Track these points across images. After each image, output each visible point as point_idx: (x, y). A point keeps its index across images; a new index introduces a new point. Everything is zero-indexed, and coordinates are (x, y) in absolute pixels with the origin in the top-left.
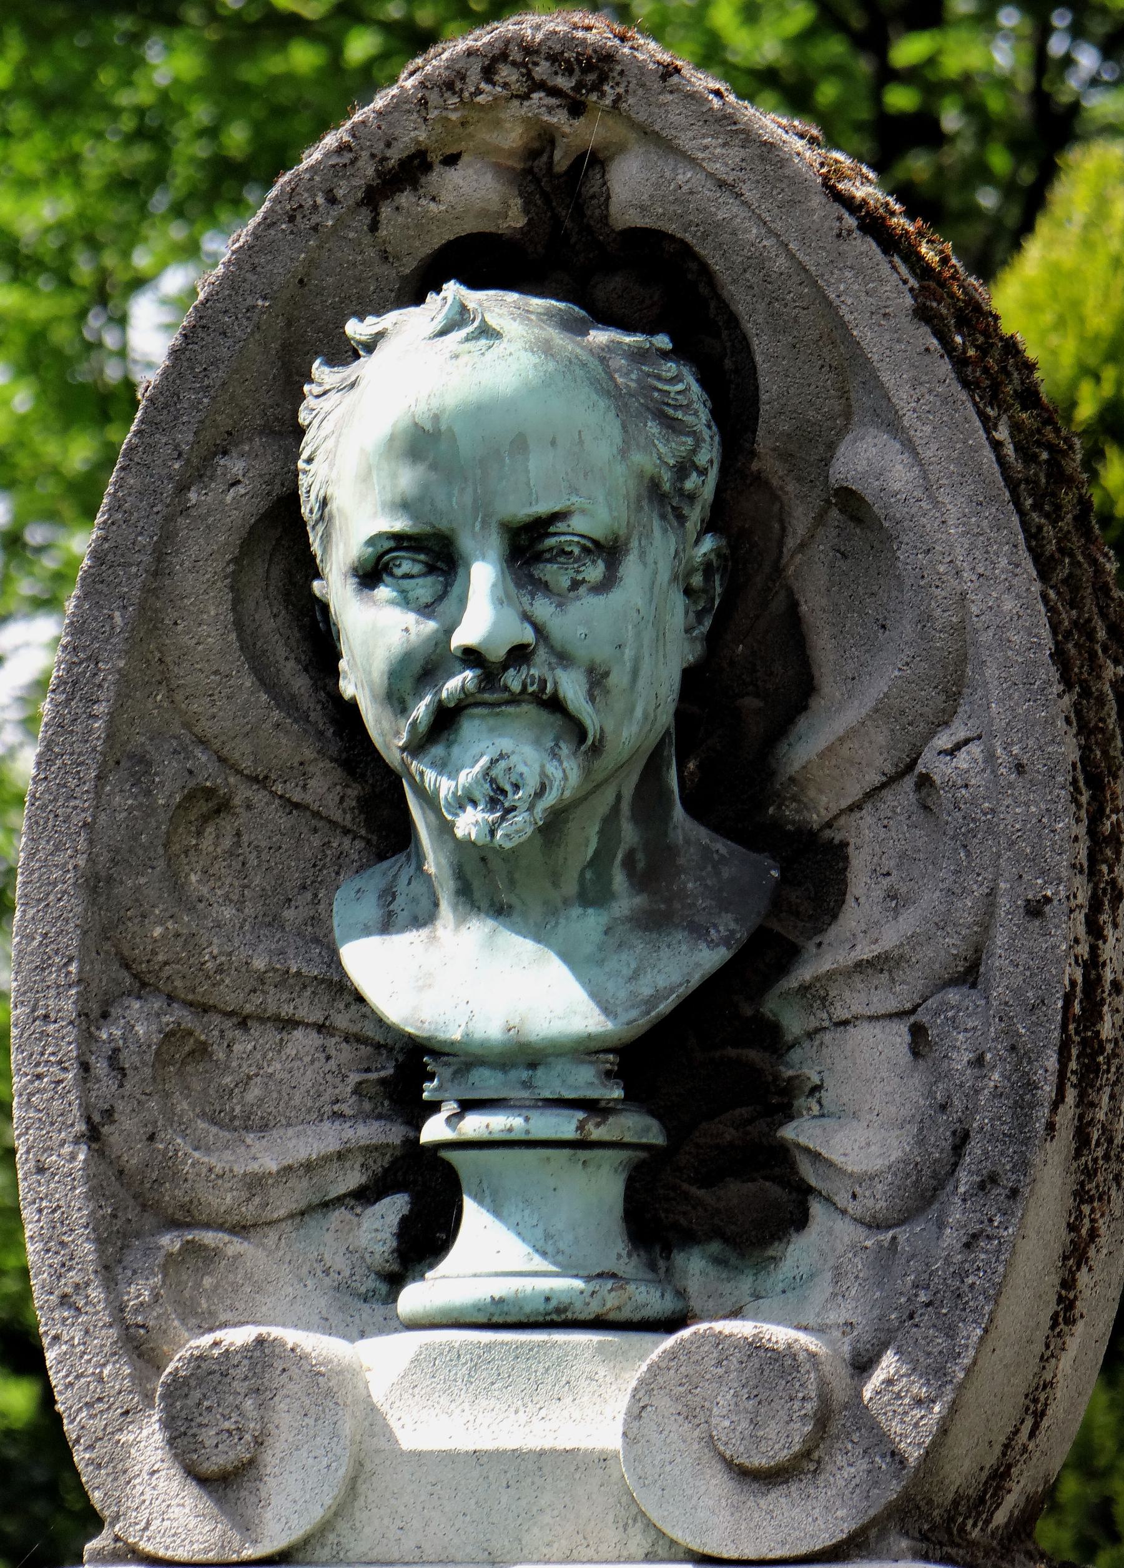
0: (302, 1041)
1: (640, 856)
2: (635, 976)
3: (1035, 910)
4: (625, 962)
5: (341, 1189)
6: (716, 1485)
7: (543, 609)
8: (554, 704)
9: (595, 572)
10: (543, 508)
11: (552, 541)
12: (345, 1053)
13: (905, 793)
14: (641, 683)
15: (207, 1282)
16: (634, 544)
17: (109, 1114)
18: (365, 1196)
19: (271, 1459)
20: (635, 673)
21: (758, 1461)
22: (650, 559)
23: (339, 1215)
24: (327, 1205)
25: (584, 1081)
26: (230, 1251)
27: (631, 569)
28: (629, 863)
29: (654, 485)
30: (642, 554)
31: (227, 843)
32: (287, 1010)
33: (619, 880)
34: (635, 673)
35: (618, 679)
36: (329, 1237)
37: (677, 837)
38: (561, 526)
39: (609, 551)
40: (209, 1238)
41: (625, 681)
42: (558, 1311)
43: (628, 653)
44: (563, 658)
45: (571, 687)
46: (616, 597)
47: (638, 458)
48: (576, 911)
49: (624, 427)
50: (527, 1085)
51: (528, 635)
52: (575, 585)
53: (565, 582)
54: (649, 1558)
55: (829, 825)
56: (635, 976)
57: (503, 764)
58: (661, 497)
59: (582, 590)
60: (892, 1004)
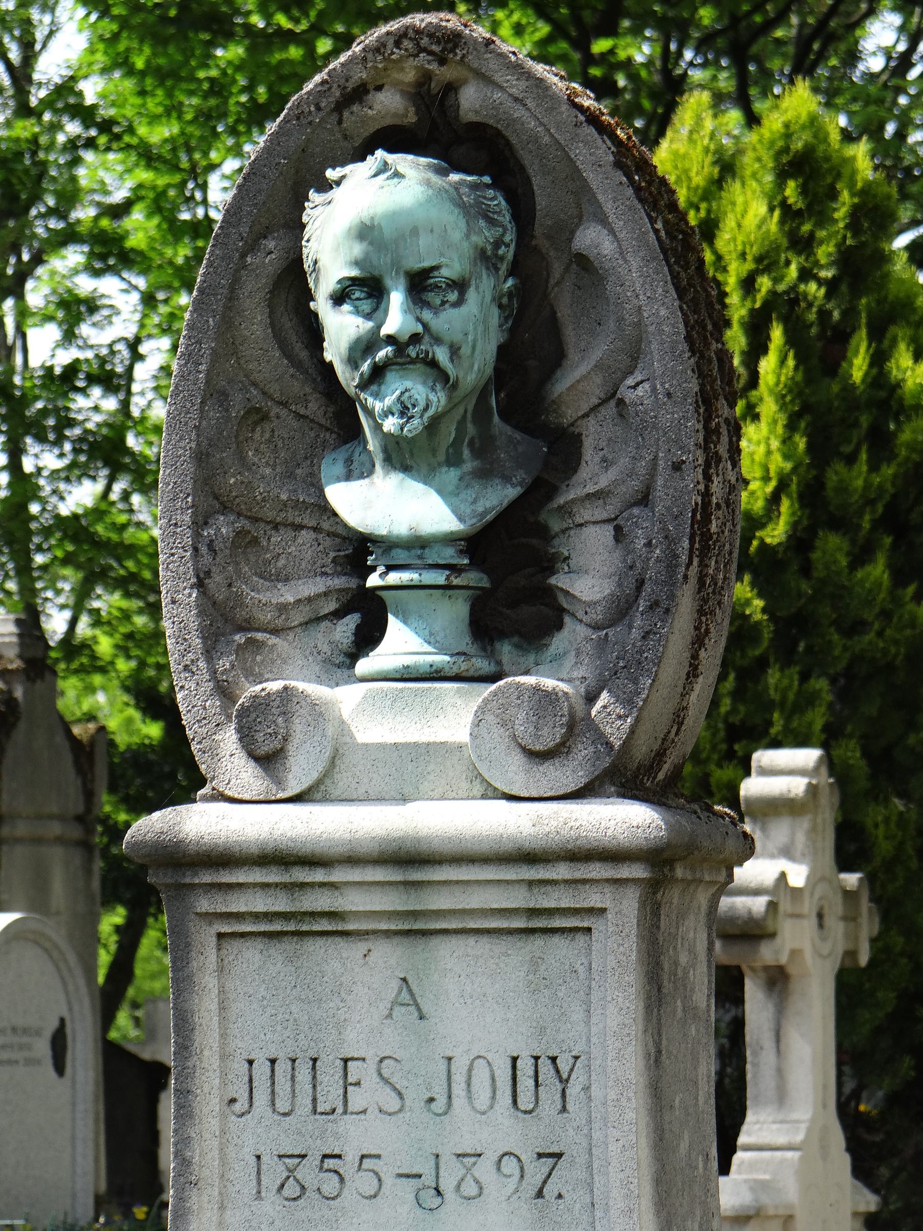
0: (306, 536)
1: (477, 440)
2: (474, 502)
3: (677, 467)
4: (469, 494)
5: (327, 611)
6: (517, 760)
7: (427, 315)
8: (433, 364)
9: (453, 296)
10: (426, 264)
11: (432, 281)
12: (328, 542)
13: (610, 409)
14: (477, 352)
15: (259, 658)
16: (473, 282)
17: (208, 573)
18: (338, 614)
19: (291, 748)
20: (474, 348)
21: (538, 747)
22: (481, 290)
23: (325, 624)
24: (319, 619)
25: (449, 555)
26: (270, 643)
27: (472, 295)
28: (471, 444)
30: (477, 288)
31: (267, 436)
32: (298, 520)
33: (466, 453)
34: (474, 348)
35: (465, 351)
36: (320, 635)
37: (496, 431)
38: (436, 273)
39: (460, 286)
40: (259, 636)
41: (469, 352)
42: (436, 672)
43: (470, 338)
44: (438, 340)
45: (442, 355)
46: (464, 309)
47: (474, 238)
48: (445, 469)
49: (467, 223)
50: (420, 557)
51: (420, 329)
52: (443, 303)
53: (438, 302)
54: (484, 797)
55: (572, 425)
56: (474, 502)
57: (407, 394)
58: (486, 258)
59: (447, 306)
60: (605, 516)
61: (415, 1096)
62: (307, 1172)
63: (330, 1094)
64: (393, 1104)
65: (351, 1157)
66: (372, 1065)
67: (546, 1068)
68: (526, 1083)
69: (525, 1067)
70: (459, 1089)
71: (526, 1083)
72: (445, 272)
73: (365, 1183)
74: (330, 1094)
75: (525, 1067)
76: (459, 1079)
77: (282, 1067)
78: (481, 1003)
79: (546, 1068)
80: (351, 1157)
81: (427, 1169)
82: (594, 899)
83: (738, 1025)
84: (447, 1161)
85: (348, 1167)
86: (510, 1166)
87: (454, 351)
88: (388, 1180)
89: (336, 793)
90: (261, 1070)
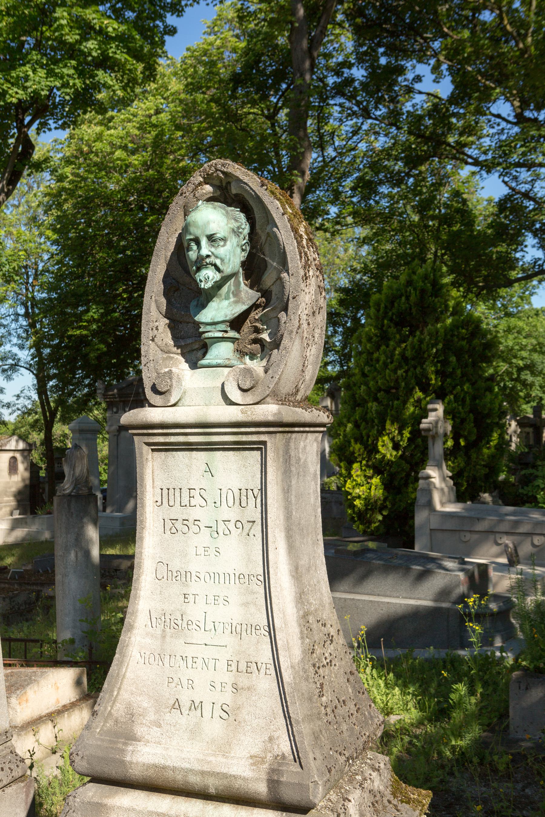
4: (231, 308)
6: (239, 392)
7: (213, 250)
8: (215, 266)
9: (222, 243)
21: (245, 388)
24: (193, 350)
25: (223, 327)
27: (228, 243)
29: (233, 230)
33: (231, 295)
35: (226, 261)
39: (224, 239)
44: (216, 257)
45: (218, 262)
46: (226, 248)
51: (210, 253)
58: (236, 232)
61: (210, 501)
62: (178, 525)
63: (185, 501)
64: (203, 503)
65: (191, 520)
66: (198, 491)
67: (250, 493)
68: (244, 498)
69: (244, 492)
70: (224, 500)
71: (244, 498)
72: (218, 235)
73: (195, 529)
74: (185, 501)
75: (244, 492)
76: (224, 497)
77: (171, 491)
78: (234, 471)
79: (250, 493)
80: (191, 520)
81: (214, 525)
82: (263, 438)
83: (290, 486)
84: (221, 523)
85: (190, 524)
86: (239, 525)
87: (222, 260)
88: (203, 528)
89: (186, 404)
90: (165, 492)
